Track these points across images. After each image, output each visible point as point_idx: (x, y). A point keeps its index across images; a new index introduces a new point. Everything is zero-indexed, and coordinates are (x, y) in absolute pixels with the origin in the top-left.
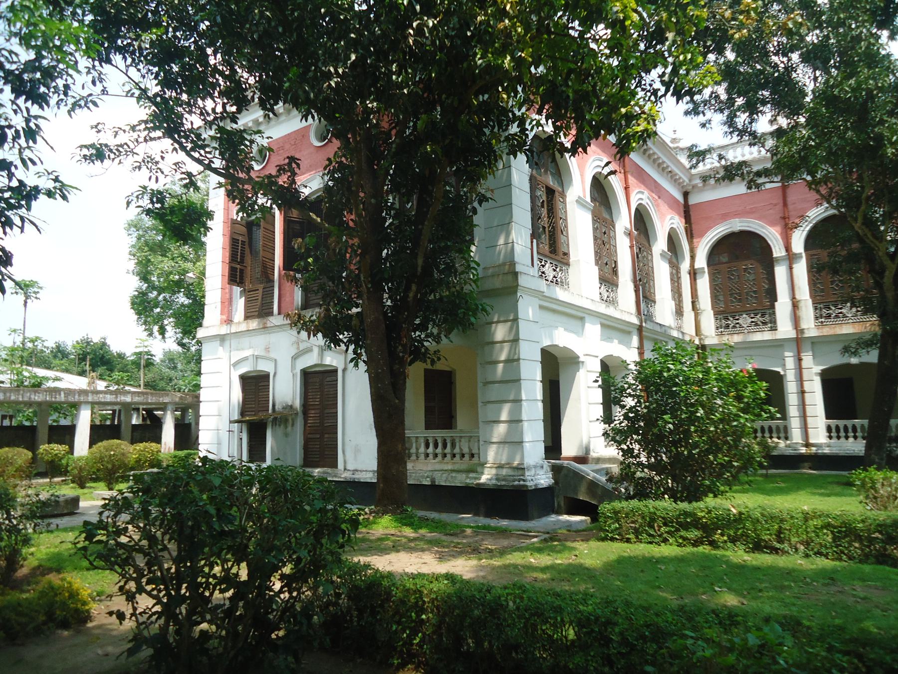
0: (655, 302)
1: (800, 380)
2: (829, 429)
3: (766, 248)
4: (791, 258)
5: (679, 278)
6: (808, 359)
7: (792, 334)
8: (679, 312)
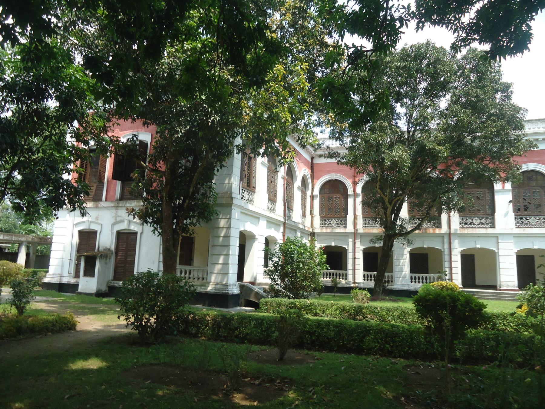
0: (293, 210)
1: (354, 253)
2: (364, 276)
3: (345, 189)
4: (356, 195)
5: (305, 199)
6: (358, 243)
7: (353, 231)
8: (304, 215)
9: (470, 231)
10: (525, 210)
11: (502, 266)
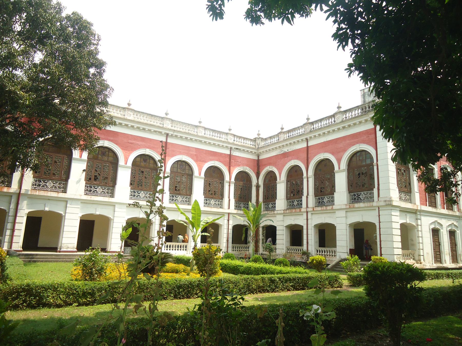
9: (42, 193)
10: (95, 180)
11: (66, 229)
